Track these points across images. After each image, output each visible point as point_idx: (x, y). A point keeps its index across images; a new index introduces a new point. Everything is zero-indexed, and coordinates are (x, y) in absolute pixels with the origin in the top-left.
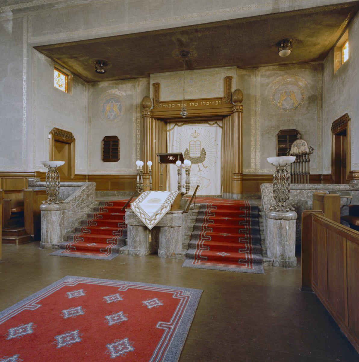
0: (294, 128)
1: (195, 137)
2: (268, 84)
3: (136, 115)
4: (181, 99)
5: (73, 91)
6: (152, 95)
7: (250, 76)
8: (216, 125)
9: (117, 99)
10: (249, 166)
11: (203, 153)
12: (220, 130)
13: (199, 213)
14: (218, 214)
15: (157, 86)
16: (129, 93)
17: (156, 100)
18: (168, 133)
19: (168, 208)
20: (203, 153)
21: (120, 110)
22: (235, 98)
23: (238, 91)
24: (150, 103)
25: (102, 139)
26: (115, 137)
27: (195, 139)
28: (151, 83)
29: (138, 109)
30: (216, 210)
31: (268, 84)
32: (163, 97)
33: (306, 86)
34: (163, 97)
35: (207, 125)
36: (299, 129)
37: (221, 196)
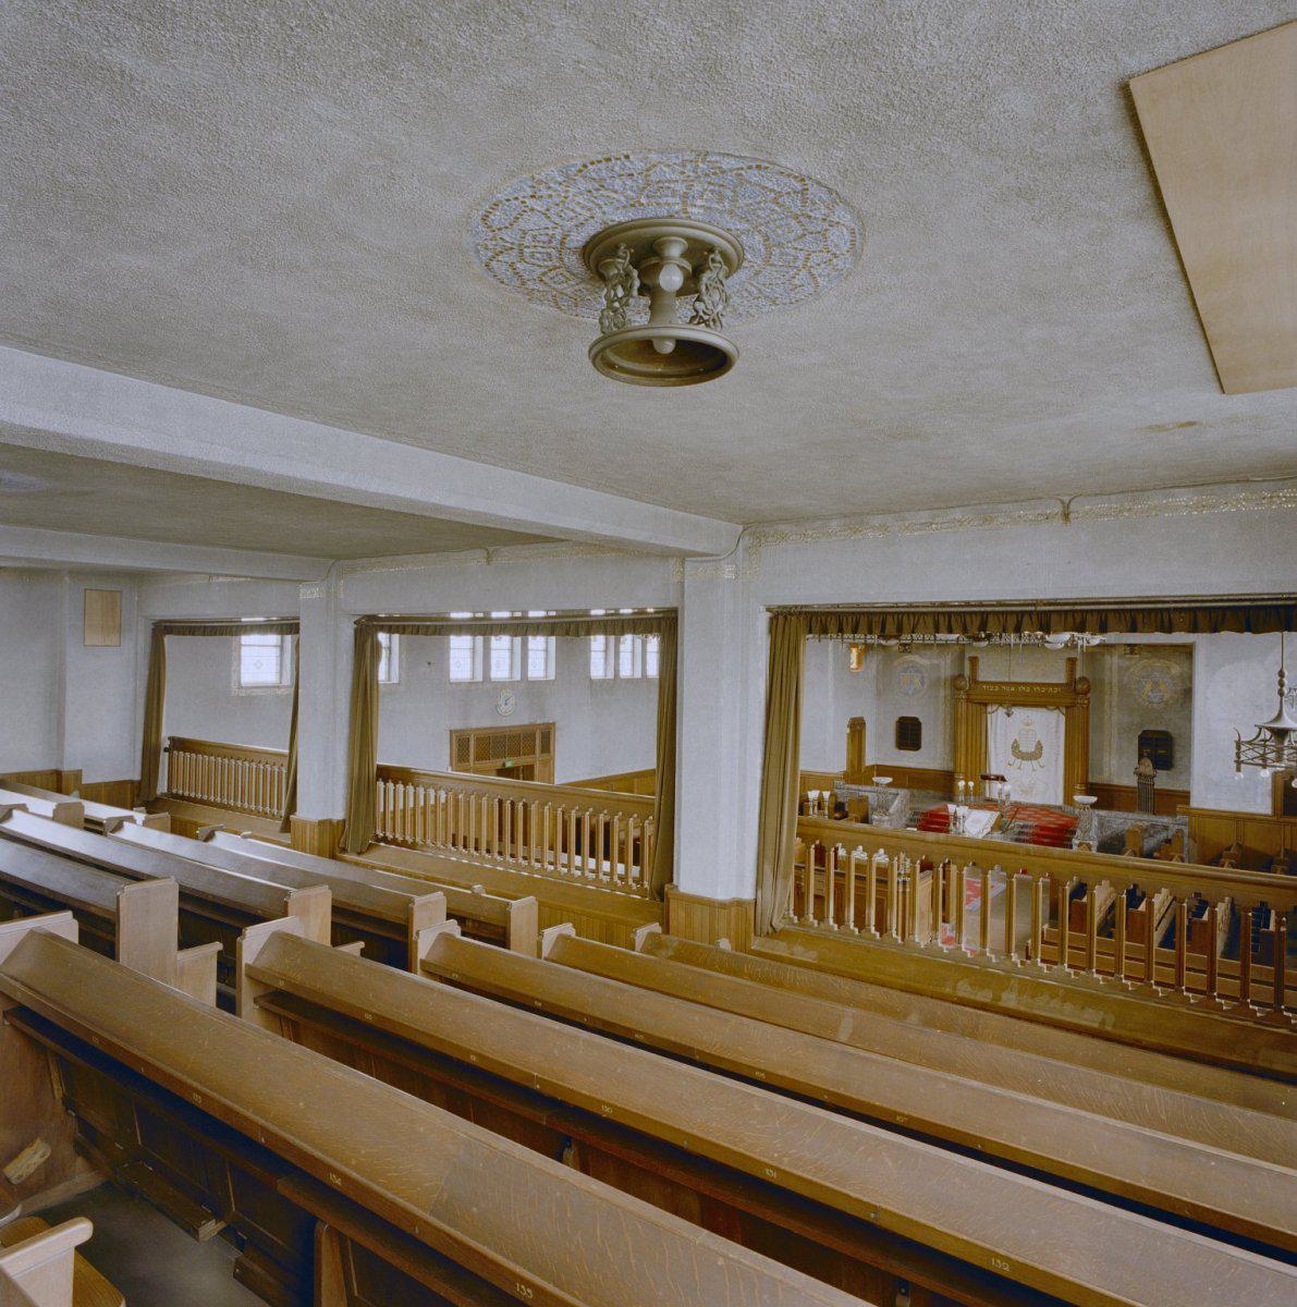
0: (1163, 729)
1: (1027, 725)
2: (1128, 668)
3: (942, 693)
4: (1007, 680)
5: (864, 665)
6: (967, 672)
7: (1103, 655)
8: (1057, 711)
9: (917, 669)
10: (1101, 772)
11: (1039, 746)
12: (1062, 719)
13: (1020, 833)
14: (1038, 835)
15: (974, 660)
16: (936, 662)
17: (974, 680)
18: (989, 716)
19: (989, 830)
20: (1039, 746)
21: (922, 683)
22: (1079, 686)
23: (1083, 679)
24: (965, 684)
25: (896, 719)
26: (915, 719)
27: (1027, 727)
28: (967, 656)
29: (948, 683)
30: (1038, 831)
31: (1128, 668)
32: (982, 677)
33: (1181, 674)
34: (982, 677)
35: (1044, 710)
36: (1169, 730)
37: (1060, 808)
